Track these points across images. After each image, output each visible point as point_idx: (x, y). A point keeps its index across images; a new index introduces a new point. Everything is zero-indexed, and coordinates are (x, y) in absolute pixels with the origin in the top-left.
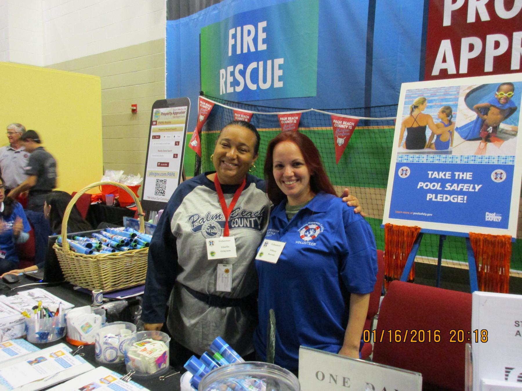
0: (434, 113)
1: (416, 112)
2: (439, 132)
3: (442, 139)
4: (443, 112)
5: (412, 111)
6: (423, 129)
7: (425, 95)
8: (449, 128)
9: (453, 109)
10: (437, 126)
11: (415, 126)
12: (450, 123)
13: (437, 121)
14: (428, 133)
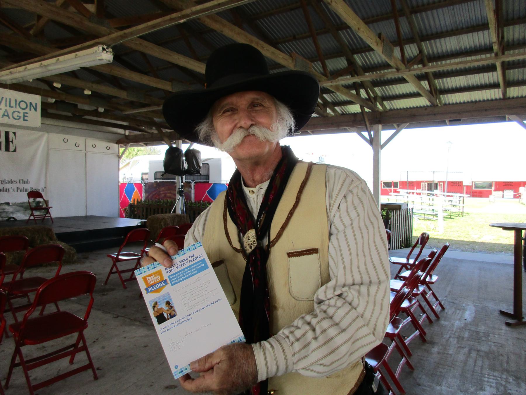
0: (163, 306)
1: (156, 309)
2: (169, 313)
3: (172, 314)
4: (167, 304)
5: (154, 309)
6: (162, 314)
7: (156, 301)
8: (172, 309)
9: (170, 301)
10: (168, 310)
11: (158, 314)
12: (172, 307)
13: (167, 308)
14: (165, 315)
